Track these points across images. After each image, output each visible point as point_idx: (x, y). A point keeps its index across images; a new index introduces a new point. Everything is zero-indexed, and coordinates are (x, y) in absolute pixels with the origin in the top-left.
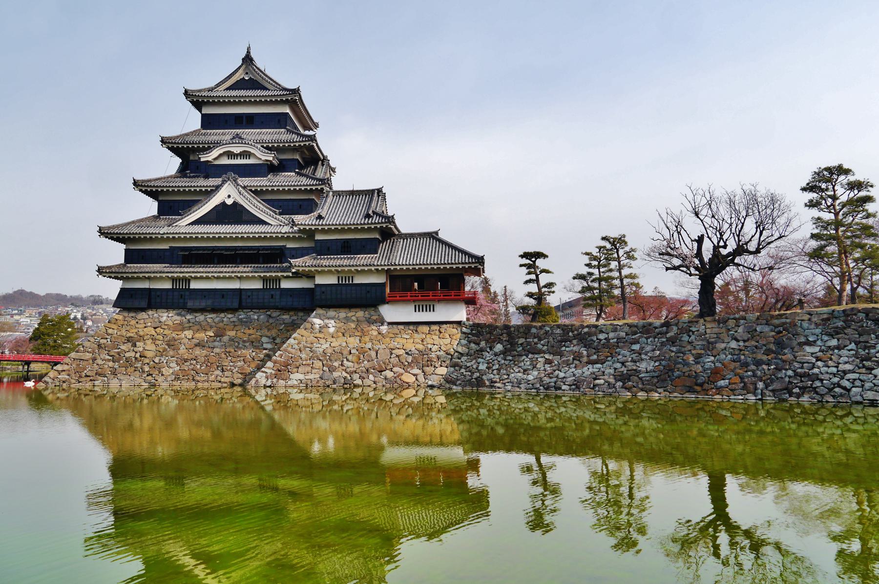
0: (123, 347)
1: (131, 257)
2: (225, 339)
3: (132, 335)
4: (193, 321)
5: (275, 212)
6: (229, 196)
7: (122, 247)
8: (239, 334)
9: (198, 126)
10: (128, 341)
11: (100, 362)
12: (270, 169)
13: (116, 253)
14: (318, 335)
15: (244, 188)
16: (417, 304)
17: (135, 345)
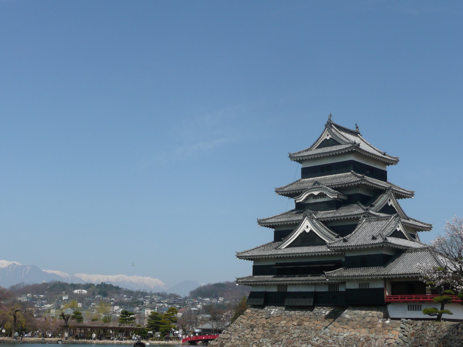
0: (247, 331)
1: (257, 270)
2: (303, 326)
3: (253, 323)
4: (287, 314)
5: (334, 235)
6: (307, 227)
7: (251, 263)
8: (311, 324)
9: (299, 176)
10: (251, 327)
11: (233, 341)
12: (336, 204)
13: (246, 269)
14: (344, 326)
15: (317, 219)
16: (410, 304)
17: (252, 330)
